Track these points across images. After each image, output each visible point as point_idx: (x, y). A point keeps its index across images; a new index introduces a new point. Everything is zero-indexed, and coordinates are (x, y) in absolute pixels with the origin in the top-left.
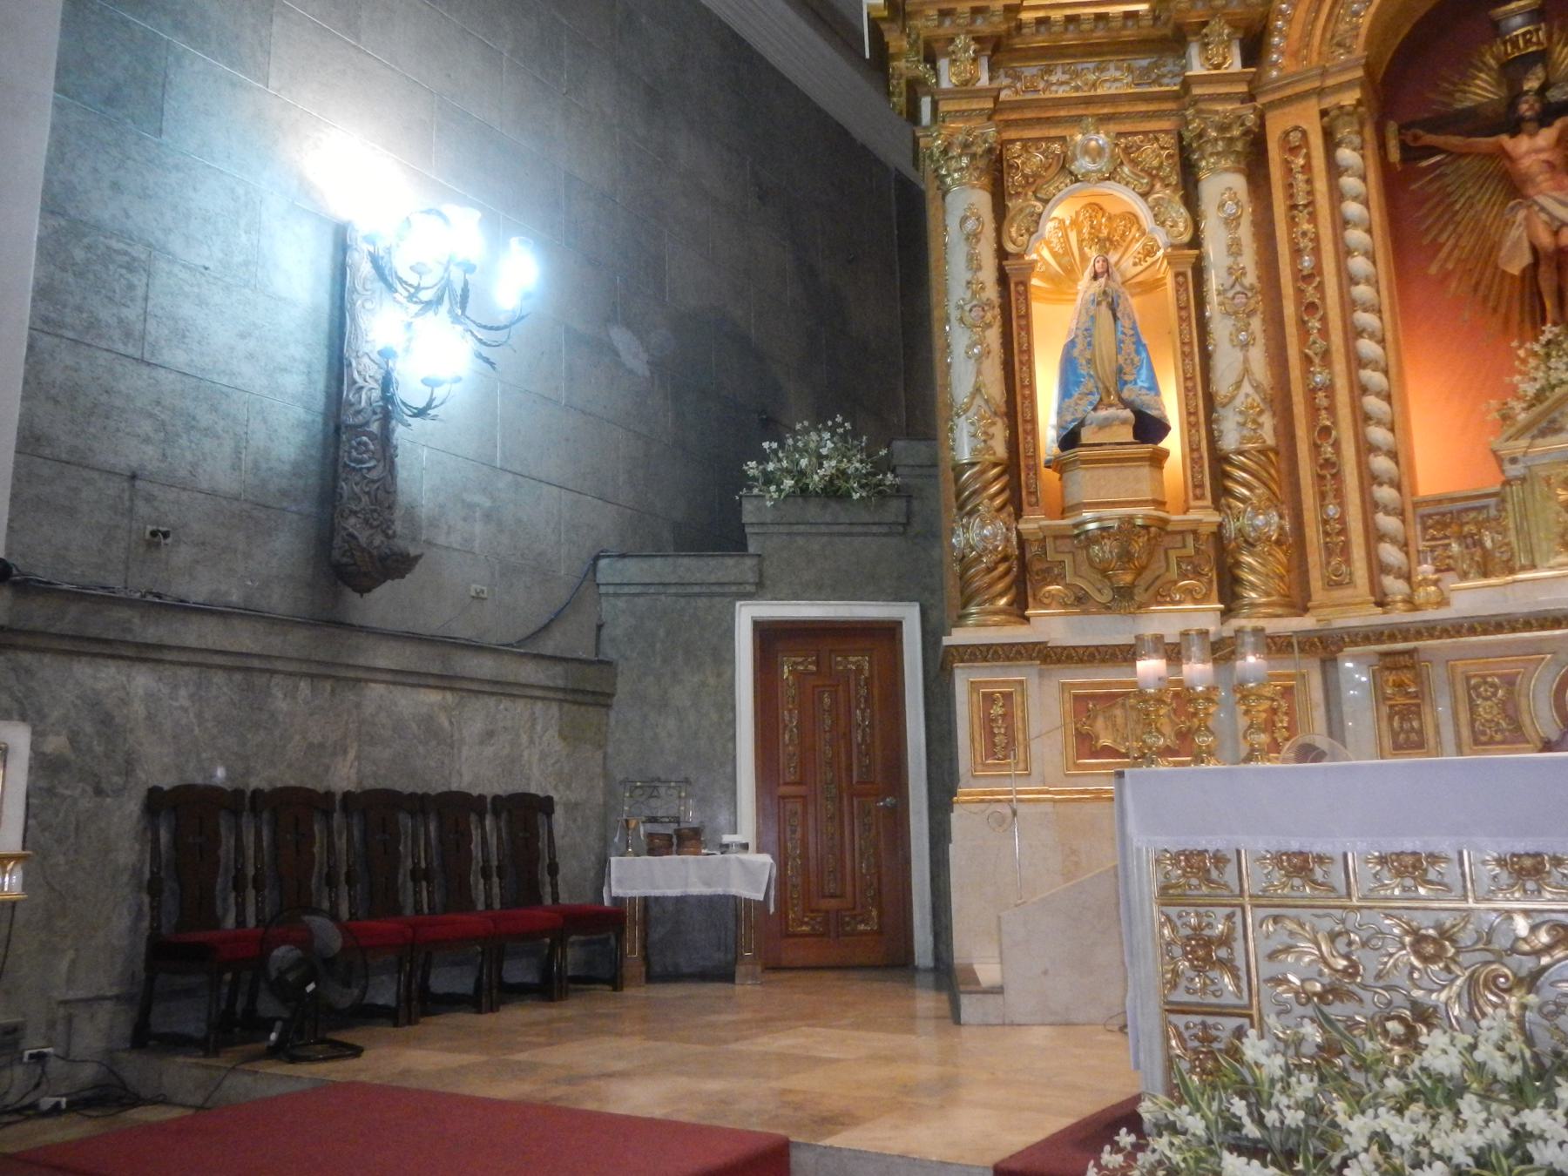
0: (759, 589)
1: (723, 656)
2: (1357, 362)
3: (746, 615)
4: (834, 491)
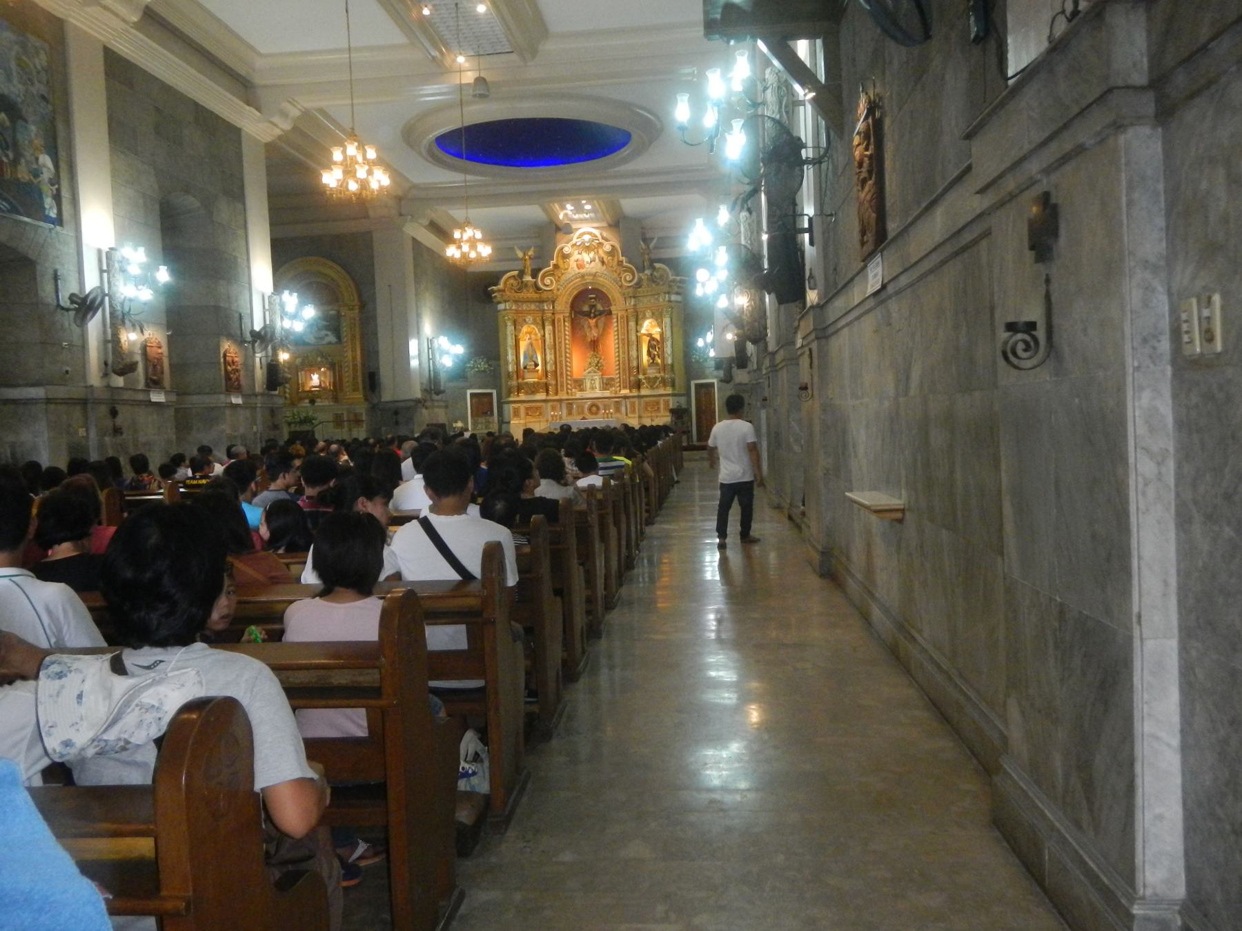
0: (470, 388)
1: (466, 399)
2: (566, 357)
3: (469, 392)
4: (483, 371)
